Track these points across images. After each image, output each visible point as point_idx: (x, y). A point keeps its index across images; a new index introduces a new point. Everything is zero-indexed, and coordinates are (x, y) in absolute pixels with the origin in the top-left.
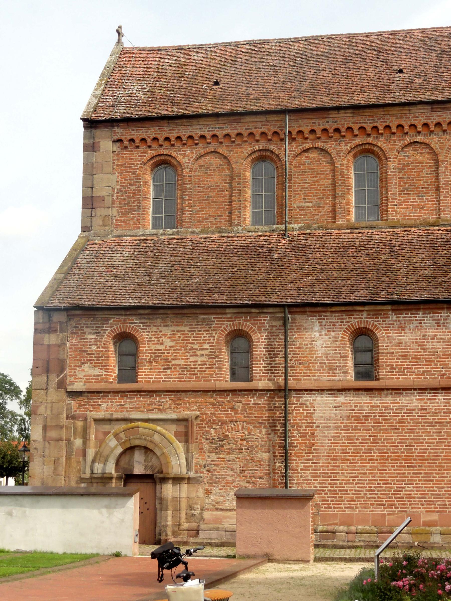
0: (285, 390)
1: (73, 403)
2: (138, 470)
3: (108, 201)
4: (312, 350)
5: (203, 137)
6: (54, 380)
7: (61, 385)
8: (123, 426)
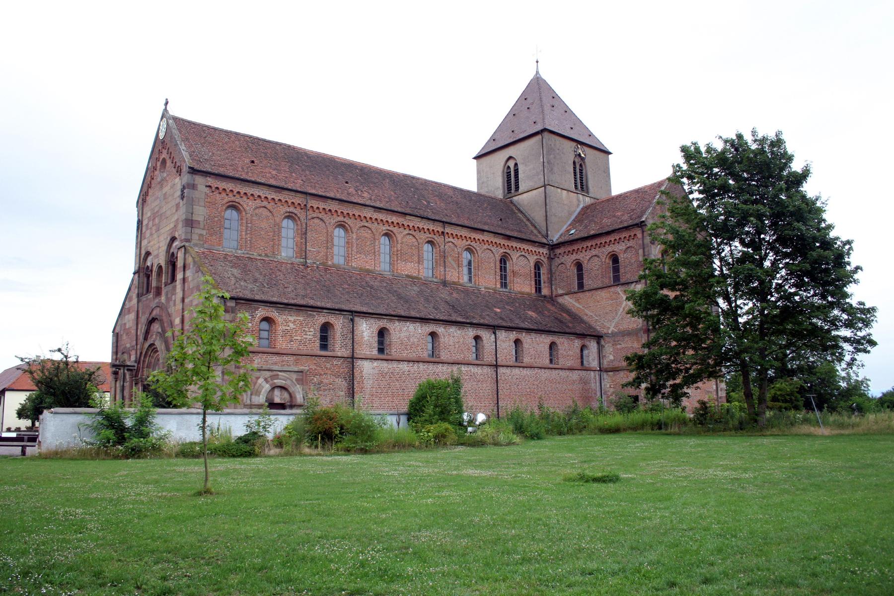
0: (353, 358)
4: (362, 337)
5: (259, 196)
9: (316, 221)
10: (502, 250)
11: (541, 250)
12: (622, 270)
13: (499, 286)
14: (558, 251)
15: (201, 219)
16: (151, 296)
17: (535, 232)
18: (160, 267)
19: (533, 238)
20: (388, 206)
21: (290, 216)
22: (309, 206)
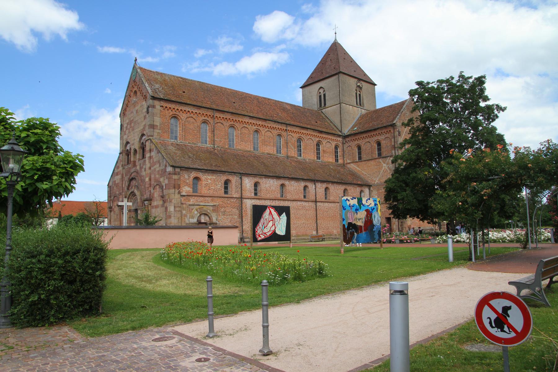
1: (182, 199)
2: (203, 221)
3: (159, 128)
5: (189, 111)
6: (177, 191)
7: (179, 193)
8: (198, 207)
9: (219, 124)
10: (318, 139)
11: (339, 139)
12: (382, 150)
13: (316, 158)
14: (347, 139)
15: (158, 124)
16: (130, 166)
17: (335, 128)
18: (135, 151)
19: (334, 132)
20: (256, 115)
21: (205, 122)
22: (215, 116)
